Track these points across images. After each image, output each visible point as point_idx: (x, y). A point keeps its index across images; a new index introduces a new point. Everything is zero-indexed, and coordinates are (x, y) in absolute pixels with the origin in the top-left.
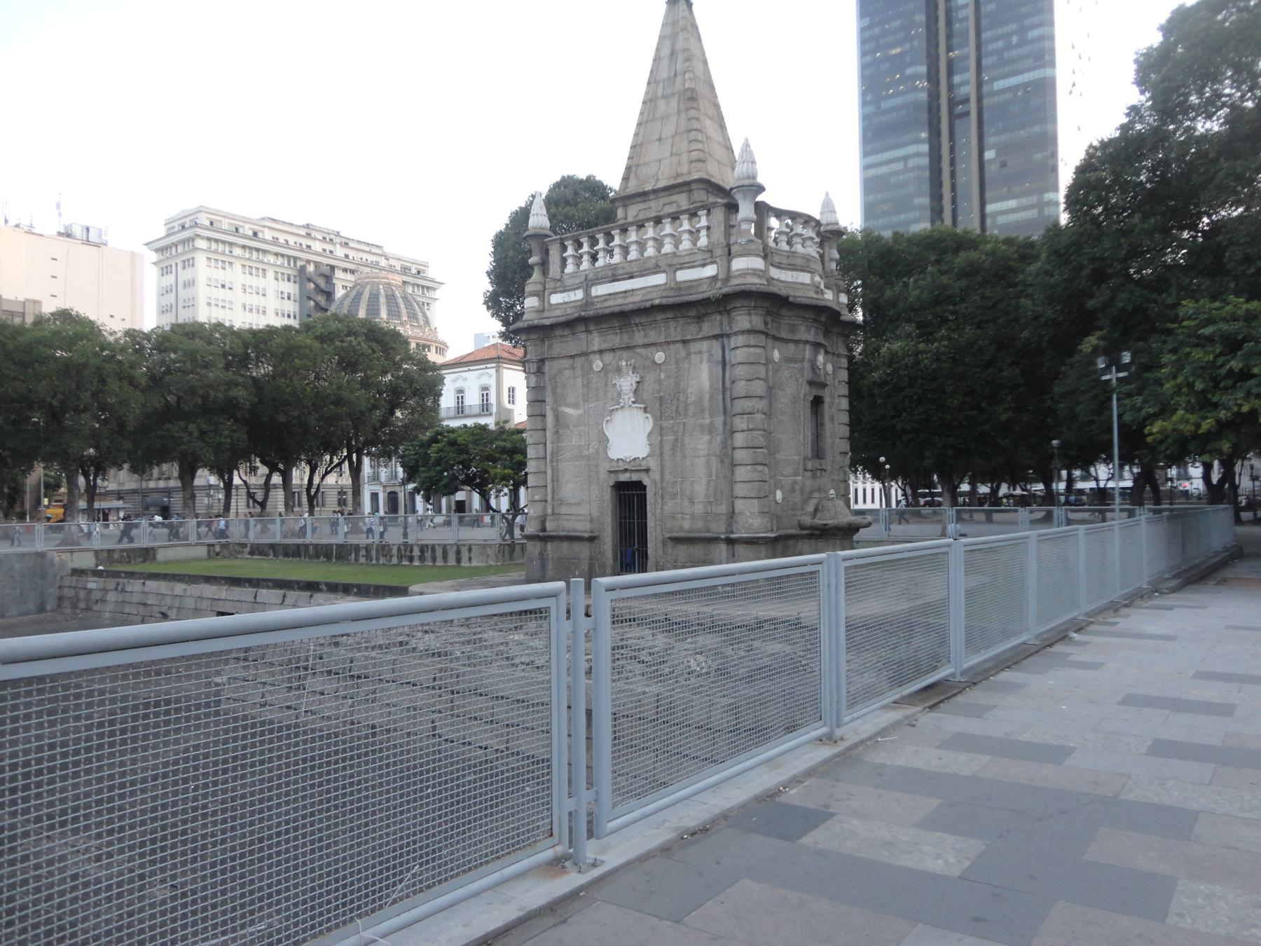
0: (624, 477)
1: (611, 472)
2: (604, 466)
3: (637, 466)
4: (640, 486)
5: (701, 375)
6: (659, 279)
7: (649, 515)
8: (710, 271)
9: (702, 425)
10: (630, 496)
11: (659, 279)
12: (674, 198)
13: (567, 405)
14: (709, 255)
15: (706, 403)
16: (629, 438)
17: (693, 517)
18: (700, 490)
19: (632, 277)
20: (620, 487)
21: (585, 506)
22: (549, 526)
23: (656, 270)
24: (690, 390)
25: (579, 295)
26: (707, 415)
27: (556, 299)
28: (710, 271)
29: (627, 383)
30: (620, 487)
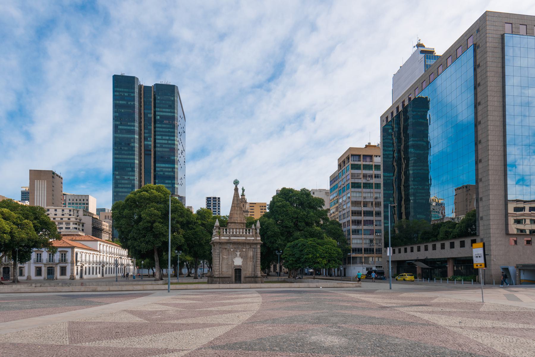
2: (233, 266)
3: (240, 266)
4: (240, 269)
5: (251, 254)
6: (244, 238)
8: (253, 238)
10: (238, 271)
11: (244, 238)
14: (253, 236)
16: (238, 262)
18: (250, 270)
21: (231, 273)
23: (244, 236)
25: (228, 238)
27: (222, 238)
28: (253, 238)
29: (238, 253)
30: (236, 269)
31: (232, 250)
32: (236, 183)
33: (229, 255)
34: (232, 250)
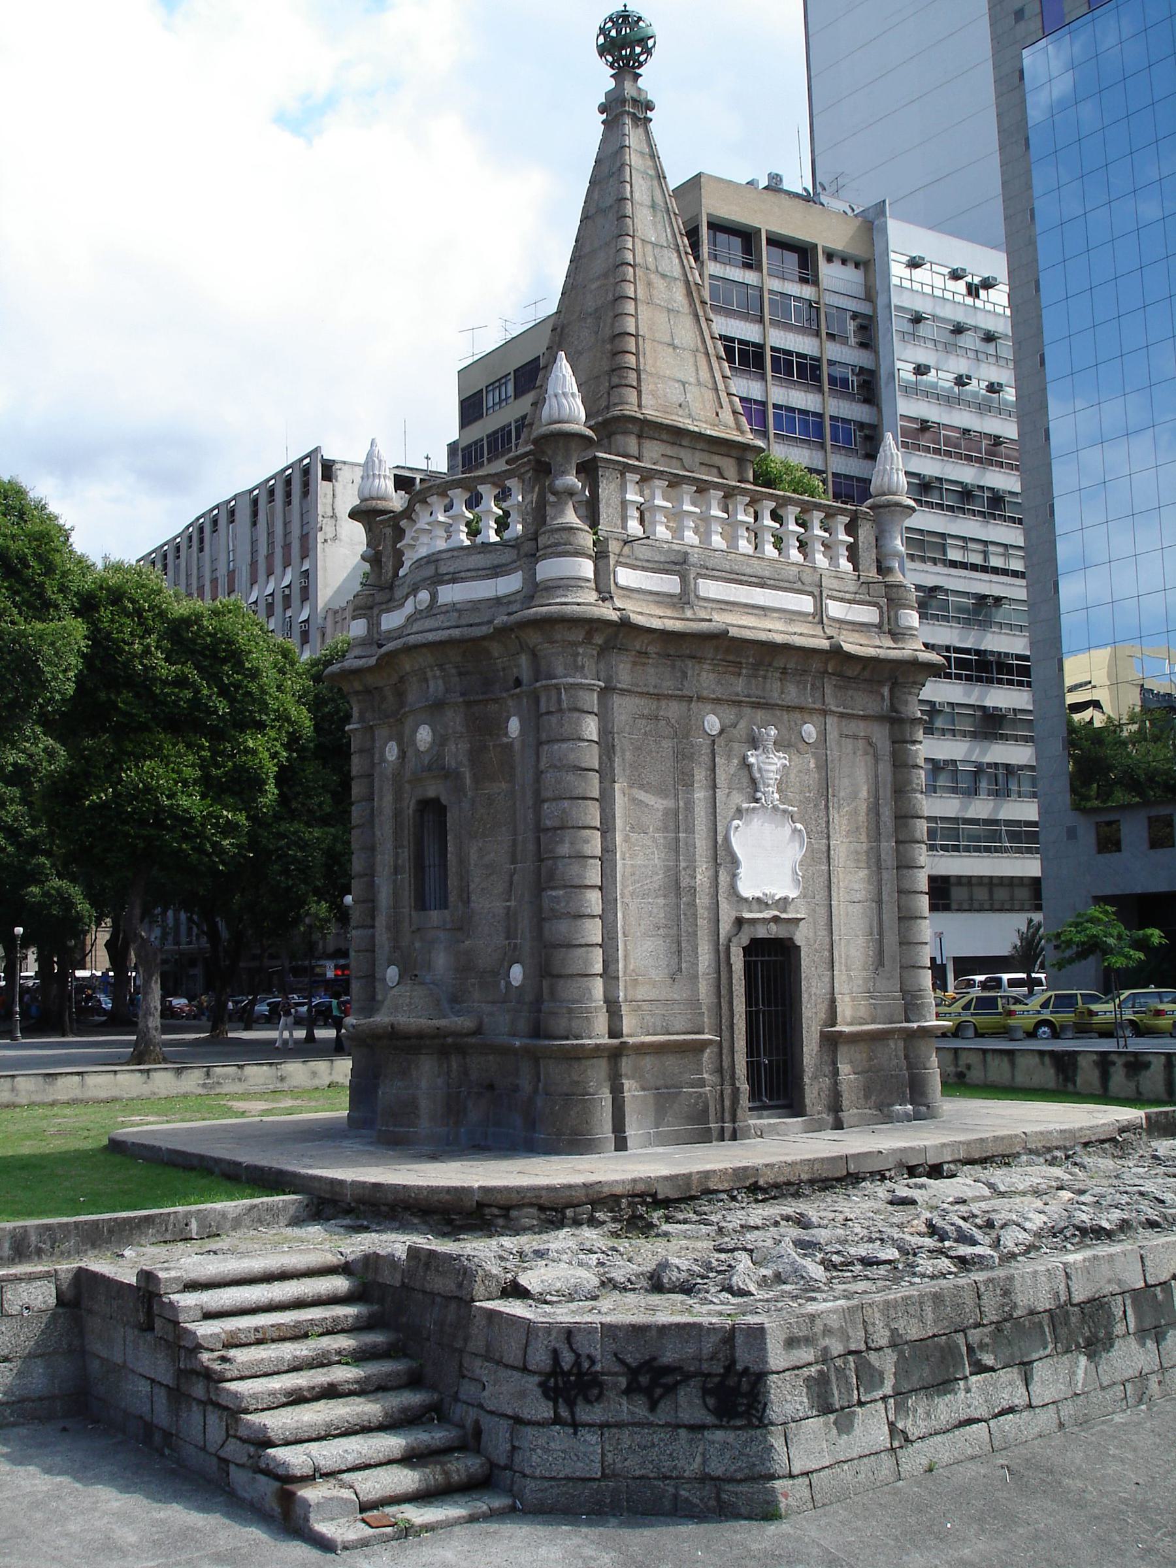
0: (761, 932)
1: (740, 922)
7: (805, 996)
8: (869, 615)
9: (857, 853)
12: (717, 460)
13: (641, 787)
15: (862, 817)
16: (768, 863)
17: (853, 999)
19: (762, 585)
20: (755, 948)
22: (628, 1024)
24: (842, 794)
26: (863, 838)
27: (625, 577)
30: (755, 948)
31: (712, 723)
32: (624, 44)
33: (685, 781)
34: (712, 723)
